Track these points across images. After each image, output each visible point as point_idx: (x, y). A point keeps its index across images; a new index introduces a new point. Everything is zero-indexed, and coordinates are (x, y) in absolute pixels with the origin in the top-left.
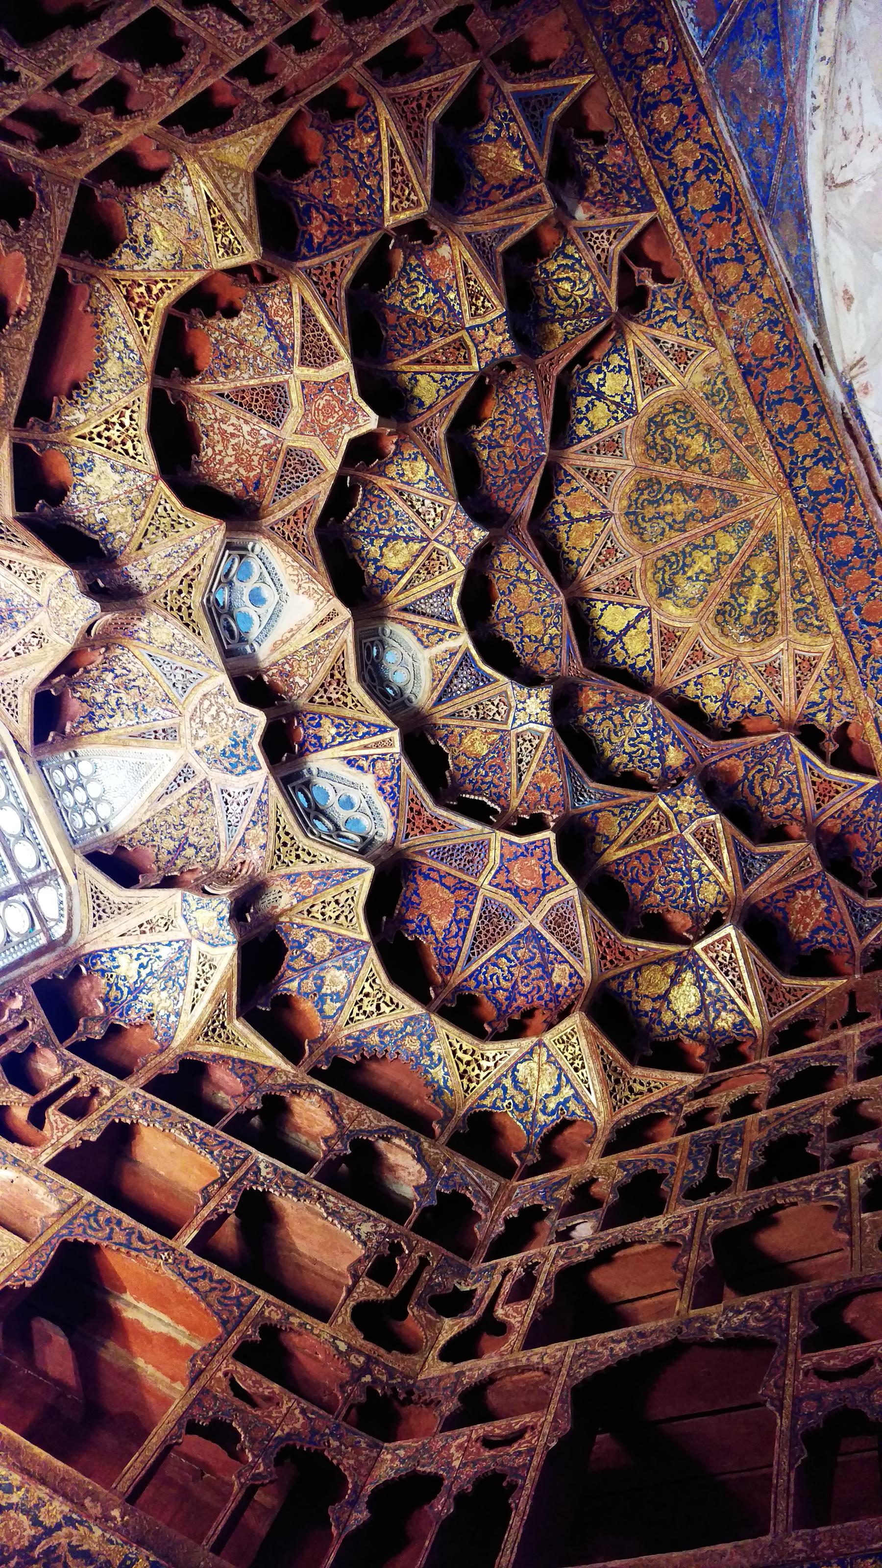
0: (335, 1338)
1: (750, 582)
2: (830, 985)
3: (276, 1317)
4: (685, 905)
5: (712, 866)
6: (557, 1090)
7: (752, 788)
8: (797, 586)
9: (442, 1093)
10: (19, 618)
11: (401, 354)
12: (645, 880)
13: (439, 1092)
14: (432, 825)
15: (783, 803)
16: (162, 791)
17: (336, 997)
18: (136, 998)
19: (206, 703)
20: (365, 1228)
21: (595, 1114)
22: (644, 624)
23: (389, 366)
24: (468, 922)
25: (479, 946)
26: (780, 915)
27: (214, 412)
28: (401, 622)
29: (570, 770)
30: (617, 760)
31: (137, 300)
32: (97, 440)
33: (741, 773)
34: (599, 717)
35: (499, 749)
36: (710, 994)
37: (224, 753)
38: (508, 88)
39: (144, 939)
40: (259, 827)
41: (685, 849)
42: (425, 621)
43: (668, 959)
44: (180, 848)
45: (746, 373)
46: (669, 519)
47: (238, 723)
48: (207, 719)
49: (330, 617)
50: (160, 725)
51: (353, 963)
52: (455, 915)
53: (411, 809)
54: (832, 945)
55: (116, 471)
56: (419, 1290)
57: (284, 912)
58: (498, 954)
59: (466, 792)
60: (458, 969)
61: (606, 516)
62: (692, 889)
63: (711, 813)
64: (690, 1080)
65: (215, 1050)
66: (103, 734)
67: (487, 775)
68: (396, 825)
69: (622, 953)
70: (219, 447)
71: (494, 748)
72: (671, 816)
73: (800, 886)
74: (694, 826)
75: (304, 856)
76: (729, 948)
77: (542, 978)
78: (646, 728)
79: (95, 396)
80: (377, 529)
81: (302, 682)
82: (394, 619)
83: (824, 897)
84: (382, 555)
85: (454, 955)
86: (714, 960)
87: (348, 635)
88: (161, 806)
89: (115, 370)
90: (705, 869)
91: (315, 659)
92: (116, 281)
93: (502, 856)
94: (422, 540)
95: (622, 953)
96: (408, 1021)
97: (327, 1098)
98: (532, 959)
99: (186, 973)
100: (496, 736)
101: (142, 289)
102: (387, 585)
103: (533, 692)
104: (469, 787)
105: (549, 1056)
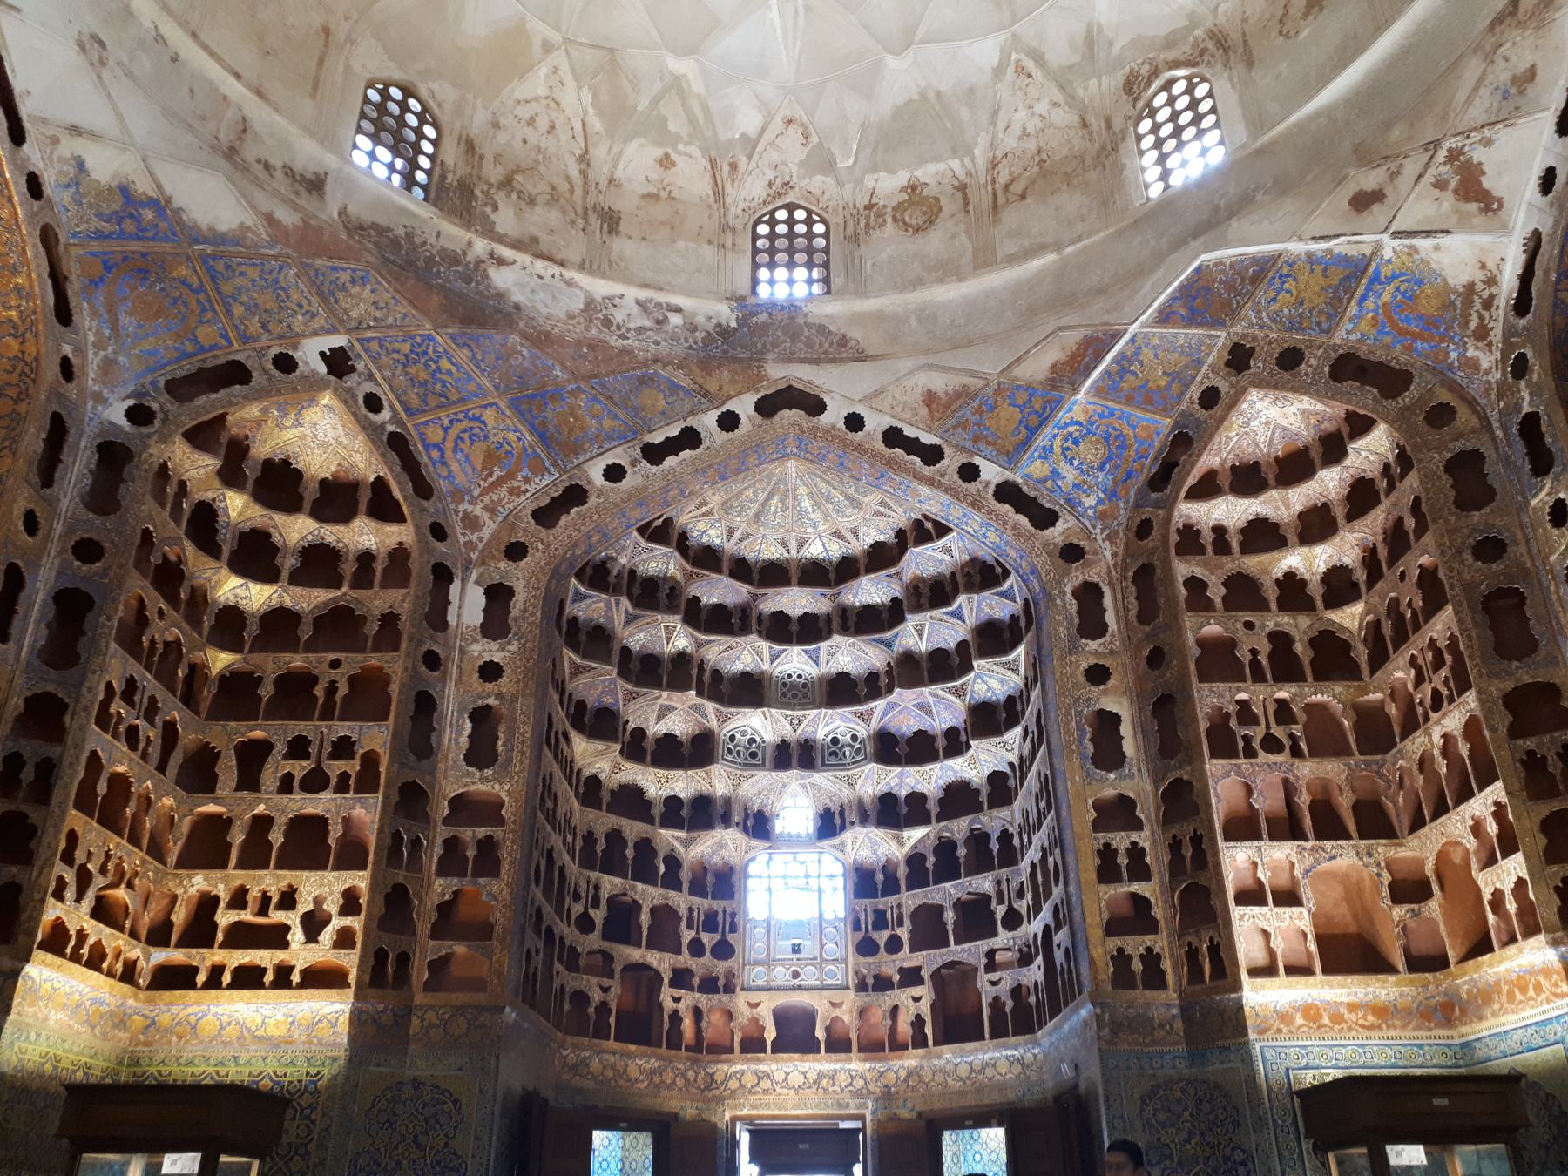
14: (870, 713)
17: (918, 782)
25: (929, 713)
29: (878, 641)
38: (567, 610)
45: (723, 478)
102: (758, 665)
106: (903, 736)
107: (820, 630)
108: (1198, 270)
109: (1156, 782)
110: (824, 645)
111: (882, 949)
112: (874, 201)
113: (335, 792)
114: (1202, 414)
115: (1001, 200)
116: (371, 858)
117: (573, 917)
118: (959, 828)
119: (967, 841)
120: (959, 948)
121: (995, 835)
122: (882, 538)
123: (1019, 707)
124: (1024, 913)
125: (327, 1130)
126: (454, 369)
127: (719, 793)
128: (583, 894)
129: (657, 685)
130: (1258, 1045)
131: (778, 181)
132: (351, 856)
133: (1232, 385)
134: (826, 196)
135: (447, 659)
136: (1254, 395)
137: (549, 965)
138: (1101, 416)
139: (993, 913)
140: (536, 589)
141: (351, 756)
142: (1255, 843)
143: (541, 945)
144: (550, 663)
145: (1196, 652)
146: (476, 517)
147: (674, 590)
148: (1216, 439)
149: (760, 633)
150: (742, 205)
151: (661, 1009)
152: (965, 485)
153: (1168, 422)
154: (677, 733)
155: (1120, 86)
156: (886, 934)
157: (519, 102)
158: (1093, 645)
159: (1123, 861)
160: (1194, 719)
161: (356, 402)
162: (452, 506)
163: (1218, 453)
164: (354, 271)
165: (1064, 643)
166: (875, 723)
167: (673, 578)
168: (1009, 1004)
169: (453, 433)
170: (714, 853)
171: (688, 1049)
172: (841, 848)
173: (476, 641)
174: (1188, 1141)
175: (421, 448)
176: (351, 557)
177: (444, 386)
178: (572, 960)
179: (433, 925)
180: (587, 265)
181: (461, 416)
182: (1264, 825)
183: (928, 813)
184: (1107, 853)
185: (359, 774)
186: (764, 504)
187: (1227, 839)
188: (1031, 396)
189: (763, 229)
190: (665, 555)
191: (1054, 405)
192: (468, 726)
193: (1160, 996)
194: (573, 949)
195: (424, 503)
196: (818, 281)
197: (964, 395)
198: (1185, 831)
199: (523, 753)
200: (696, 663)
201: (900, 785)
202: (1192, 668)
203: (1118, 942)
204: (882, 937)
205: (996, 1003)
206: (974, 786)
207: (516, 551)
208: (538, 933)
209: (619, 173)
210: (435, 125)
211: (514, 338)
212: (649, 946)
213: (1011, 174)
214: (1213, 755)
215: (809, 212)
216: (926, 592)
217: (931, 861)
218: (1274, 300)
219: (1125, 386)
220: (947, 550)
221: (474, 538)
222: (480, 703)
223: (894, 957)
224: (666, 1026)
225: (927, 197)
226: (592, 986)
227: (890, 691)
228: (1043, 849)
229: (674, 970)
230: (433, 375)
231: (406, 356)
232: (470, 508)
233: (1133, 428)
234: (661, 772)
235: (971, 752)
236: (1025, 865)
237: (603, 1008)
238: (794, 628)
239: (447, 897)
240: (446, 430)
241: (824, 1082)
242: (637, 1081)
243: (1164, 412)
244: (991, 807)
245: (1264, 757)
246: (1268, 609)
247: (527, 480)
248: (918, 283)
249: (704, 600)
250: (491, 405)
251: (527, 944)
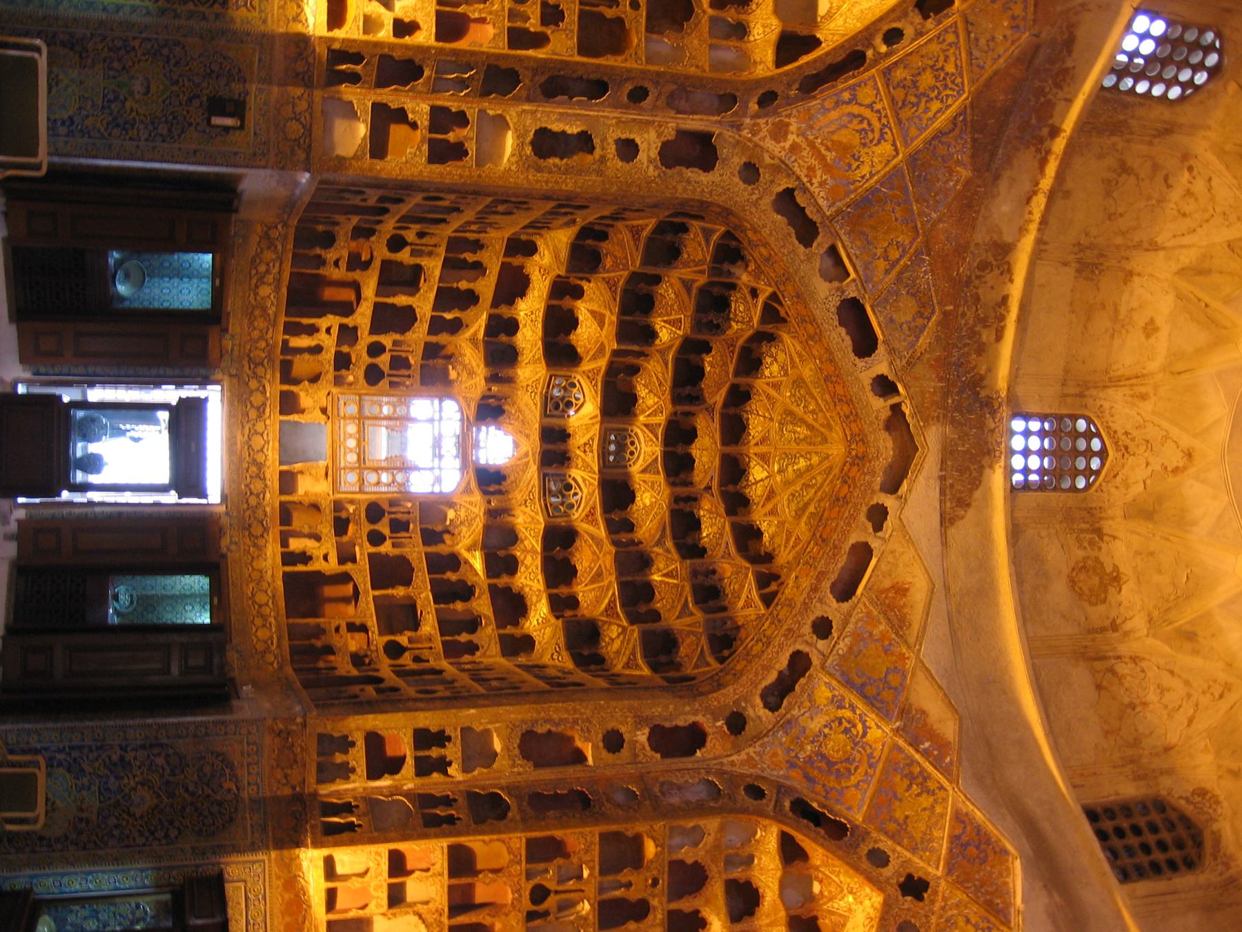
1: (812, 486)
8: (819, 501)
11: (659, 316)
14: (593, 522)
22: (766, 482)
23: (652, 320)
25: (593, 581)
26: (680, 640)
28: (641, 430)
29: (664, 529)
38: (695, 223)
39: (470, 507)
42: (650, 435)
46: (797, 435)
49: (596, 417)
50: (527, 432)
58: (594, 589)
61: (771, 419)
73: (693, 633)
87: (598, 426)
88: (519, 462)
96: (539, 590)
102: (643, 411)
106: (572, 554)
107: (677, 474)
108: (1006, 852)
109: (509, 789)
110: (661, 478)
111: (372, 527)
112: (1106, 538)
113: (510, 10)
114: (864, 849)
115: (1099, 665)
116: (448, 46)
117: (402, 232)
118: (482, 605)
119: (469, 612)
120: (371, 598)
121: (474, 638)
122: (766, 537)
123: (593, 667)
124: (401, 661)
125: (204, 18)
126: (930, 115)
128: (424, 241)
129: (624, 310)
130: (265, 857)
131: (1128, 442)
132: (450, 26)
133: (888, 879)
134: (1113, 490)
135: (642, 109)
136: (878, 899)
137: (356, 210)
138: (870, 756)
139: (401, 633)
140: (711, 193)
141: (545, 21)
142: (446, 872)
143: (372, 202)
144: (637, 206)
145: (630, 834)
146: (786, 134)
147: (717, 329)
148: (837, 862)
149: (675, 414)
150: (1106, 405)
151: (320, 316)
152: (809, 622)
153: (859, 818)
154: (579, 330)
155: (1203, 785)
156: (386, 531)
157: (1210, 180)
158: (642, 736)
159: (435, 752)
160: (563, 827)
161: (894, 21)
162: (795, 112)
163: (826, 864)
164: (1024, 19)
165: (647, 713)
166: (583, 527)
167: (730, 327)
168: (319, 644)
169: (867, 113)
170: (465, 366)
171: (285, 342)
172: (467, 491)
173: (659, 135)
174: (187, 790)
175: (851, 82)
176: (743, 17)
177: (913, 105)
178: (364, 232)
179: (386, 105)
180: (1042, 247)
181: (884, 121)
182: (464, 881)
183: (497, 576)
184: (441, 739)
185: (527, 31)
186: (803, 421)
187: (450, 847)
188: (896, 689)
189: (1081, 425)
190: (751, 319)
191: (884, 713)
192: (573, 130)
193: (312, 779)
194: (371, 232)
195: (797, 86)
196: (1026, 480)
197: (900, 623)
198: (460, 811)
199: (547, 182)
200: (645, 349)
201: (525, 551)
202: (614, 828)
203: (361, 743)
204: (384, 527)
205: (320, 631)
206: (522, 621)
207: (750, 172)
208: (382, 199)
209: (1136, 279)
210: (1182, 98)
211: (965, 173)
212: (377, 306)
213: (1124, 676)
214: (530, 843)
215: (1097, 473)
216: (710, 581)
217: (451, 576)
218: (968, 921)
219: (897, 779)
220: (748, 605)
221: (764, 132)
222: (596, 141)
223: (365, 538)
224: (306, 321)
225: (1106, 592)
226: (341, 251)
227: (615, 543)
228: (453, 682)
229: (355, 328)
230: (924, 94)
231: (942, 69)
232: (793, 128)
233: (857, 786)
234: (540, 315)
235: (553, 620)
236: (444, 664)
237: (321, 262)
238: (680, 449)
239: (410, 116)
240: (870, 106)
241: (254, 469)
242: (256, 294)
243: (868, 818)
244: (501, 637)
245: (527, 887)
246: (669, 901)
247: (822, 184)
248: (1019, 580)
249: (708, 359)
250: (896, 150)
251: (367, 190)
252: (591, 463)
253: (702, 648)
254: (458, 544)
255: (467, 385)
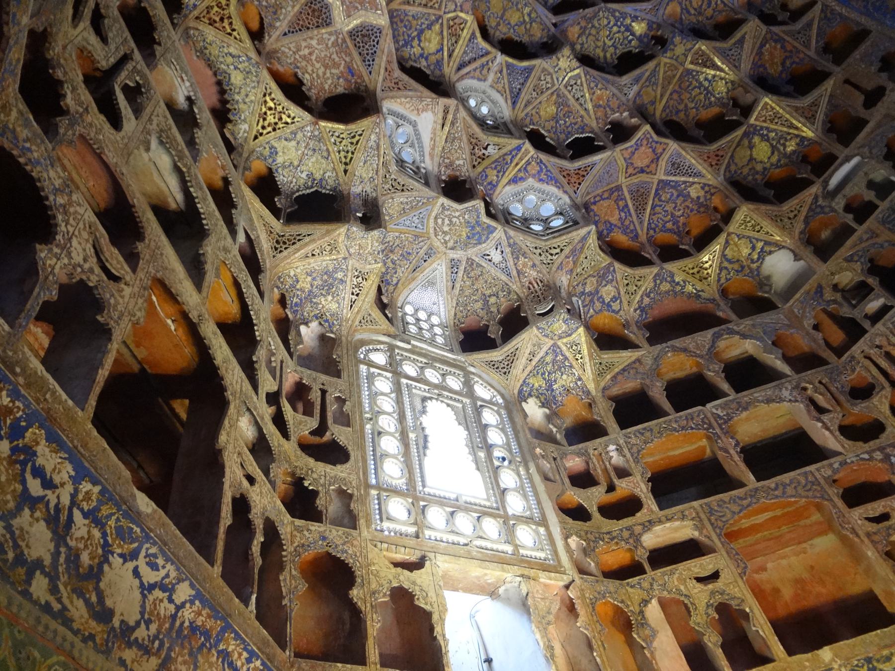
0: (858, 456)
2: (828, 86)
3: (829, 473)
4: (711, 103)
5: (713, 72)
6: (754, 248)
7: (688, 12)
9: (700, 296)
10: (339, 275)
12: (681, 107)
13: (698, 296)
15: (709, 7)
16: (450, 284)
17: (615, 299)
18: (553, 390)
19: (440, 221)
20: (786, 393)
21: (783, 244)
24: (627, 206)
25: (640, 209)
26: (761, 69)
27: (290, 49)
28: (462, 78)
29: (608, 81)
30: (608, 55)
31: (217, 19)
32: (265, 132)
33: (679, 10)
34: (584, 38)
35: (562, 103)
36: (773, 139)
37: (468, 237)
40: (522, 259)
41: (691, 74)
43: (741, 139)
44: (486, 302)
47: (466, 217)
48: (446, 229)
49: (446, 112)
50: (422, 252)
51: (610, 277)
52: (619, 208)
53: (564, 177)
54: (797, 63)
55: (290, 140)
56: (842, 398)
57: (569, 286)
58: (653, 208)
59: (565, 141)
60: (640, 232)
62: (708, 92)
63: (695, 45)
64: (814, 189)
65: (608, 377)
66: (399, 285)
67: (566, 122)
68: (565, 192)
69: (717, 156)
70: (310, 69)
71: (558, 104)
72: (674, 62)
73: (762, 46)
74: (689, 59)
75: (554, 251)
76: (770, 109)
77: (684, 201)
78: (612, 23)
79: (241, 106)
80: (409, 36)
81: (461, 162)
82: (458, 80)
83: (776, 41)
84: (422, 49)
85: (632, 227)
86: (764, 121)
88: (456, 291)
89: (239, 78)
90: (710, 77)
91: (456, 143)
92: (197, 18)
93: (625, 159)
94: (437, 20)
95: (717, 156)
97: (674, 349)
98: (672, 195)
99: (566, 358)
100: (554, 97)
101: (216, 9)
102: (439, 63)
103: (559, 55)
104: (562, 136)
105: (738, 236)
127: (357, 189)
170: (310, 296)
252: (504, 151)
253: (784, 32)
254: (588, 393)
255: (347, 302)
